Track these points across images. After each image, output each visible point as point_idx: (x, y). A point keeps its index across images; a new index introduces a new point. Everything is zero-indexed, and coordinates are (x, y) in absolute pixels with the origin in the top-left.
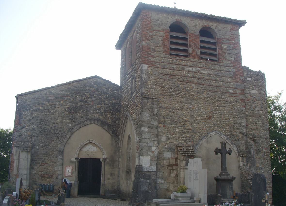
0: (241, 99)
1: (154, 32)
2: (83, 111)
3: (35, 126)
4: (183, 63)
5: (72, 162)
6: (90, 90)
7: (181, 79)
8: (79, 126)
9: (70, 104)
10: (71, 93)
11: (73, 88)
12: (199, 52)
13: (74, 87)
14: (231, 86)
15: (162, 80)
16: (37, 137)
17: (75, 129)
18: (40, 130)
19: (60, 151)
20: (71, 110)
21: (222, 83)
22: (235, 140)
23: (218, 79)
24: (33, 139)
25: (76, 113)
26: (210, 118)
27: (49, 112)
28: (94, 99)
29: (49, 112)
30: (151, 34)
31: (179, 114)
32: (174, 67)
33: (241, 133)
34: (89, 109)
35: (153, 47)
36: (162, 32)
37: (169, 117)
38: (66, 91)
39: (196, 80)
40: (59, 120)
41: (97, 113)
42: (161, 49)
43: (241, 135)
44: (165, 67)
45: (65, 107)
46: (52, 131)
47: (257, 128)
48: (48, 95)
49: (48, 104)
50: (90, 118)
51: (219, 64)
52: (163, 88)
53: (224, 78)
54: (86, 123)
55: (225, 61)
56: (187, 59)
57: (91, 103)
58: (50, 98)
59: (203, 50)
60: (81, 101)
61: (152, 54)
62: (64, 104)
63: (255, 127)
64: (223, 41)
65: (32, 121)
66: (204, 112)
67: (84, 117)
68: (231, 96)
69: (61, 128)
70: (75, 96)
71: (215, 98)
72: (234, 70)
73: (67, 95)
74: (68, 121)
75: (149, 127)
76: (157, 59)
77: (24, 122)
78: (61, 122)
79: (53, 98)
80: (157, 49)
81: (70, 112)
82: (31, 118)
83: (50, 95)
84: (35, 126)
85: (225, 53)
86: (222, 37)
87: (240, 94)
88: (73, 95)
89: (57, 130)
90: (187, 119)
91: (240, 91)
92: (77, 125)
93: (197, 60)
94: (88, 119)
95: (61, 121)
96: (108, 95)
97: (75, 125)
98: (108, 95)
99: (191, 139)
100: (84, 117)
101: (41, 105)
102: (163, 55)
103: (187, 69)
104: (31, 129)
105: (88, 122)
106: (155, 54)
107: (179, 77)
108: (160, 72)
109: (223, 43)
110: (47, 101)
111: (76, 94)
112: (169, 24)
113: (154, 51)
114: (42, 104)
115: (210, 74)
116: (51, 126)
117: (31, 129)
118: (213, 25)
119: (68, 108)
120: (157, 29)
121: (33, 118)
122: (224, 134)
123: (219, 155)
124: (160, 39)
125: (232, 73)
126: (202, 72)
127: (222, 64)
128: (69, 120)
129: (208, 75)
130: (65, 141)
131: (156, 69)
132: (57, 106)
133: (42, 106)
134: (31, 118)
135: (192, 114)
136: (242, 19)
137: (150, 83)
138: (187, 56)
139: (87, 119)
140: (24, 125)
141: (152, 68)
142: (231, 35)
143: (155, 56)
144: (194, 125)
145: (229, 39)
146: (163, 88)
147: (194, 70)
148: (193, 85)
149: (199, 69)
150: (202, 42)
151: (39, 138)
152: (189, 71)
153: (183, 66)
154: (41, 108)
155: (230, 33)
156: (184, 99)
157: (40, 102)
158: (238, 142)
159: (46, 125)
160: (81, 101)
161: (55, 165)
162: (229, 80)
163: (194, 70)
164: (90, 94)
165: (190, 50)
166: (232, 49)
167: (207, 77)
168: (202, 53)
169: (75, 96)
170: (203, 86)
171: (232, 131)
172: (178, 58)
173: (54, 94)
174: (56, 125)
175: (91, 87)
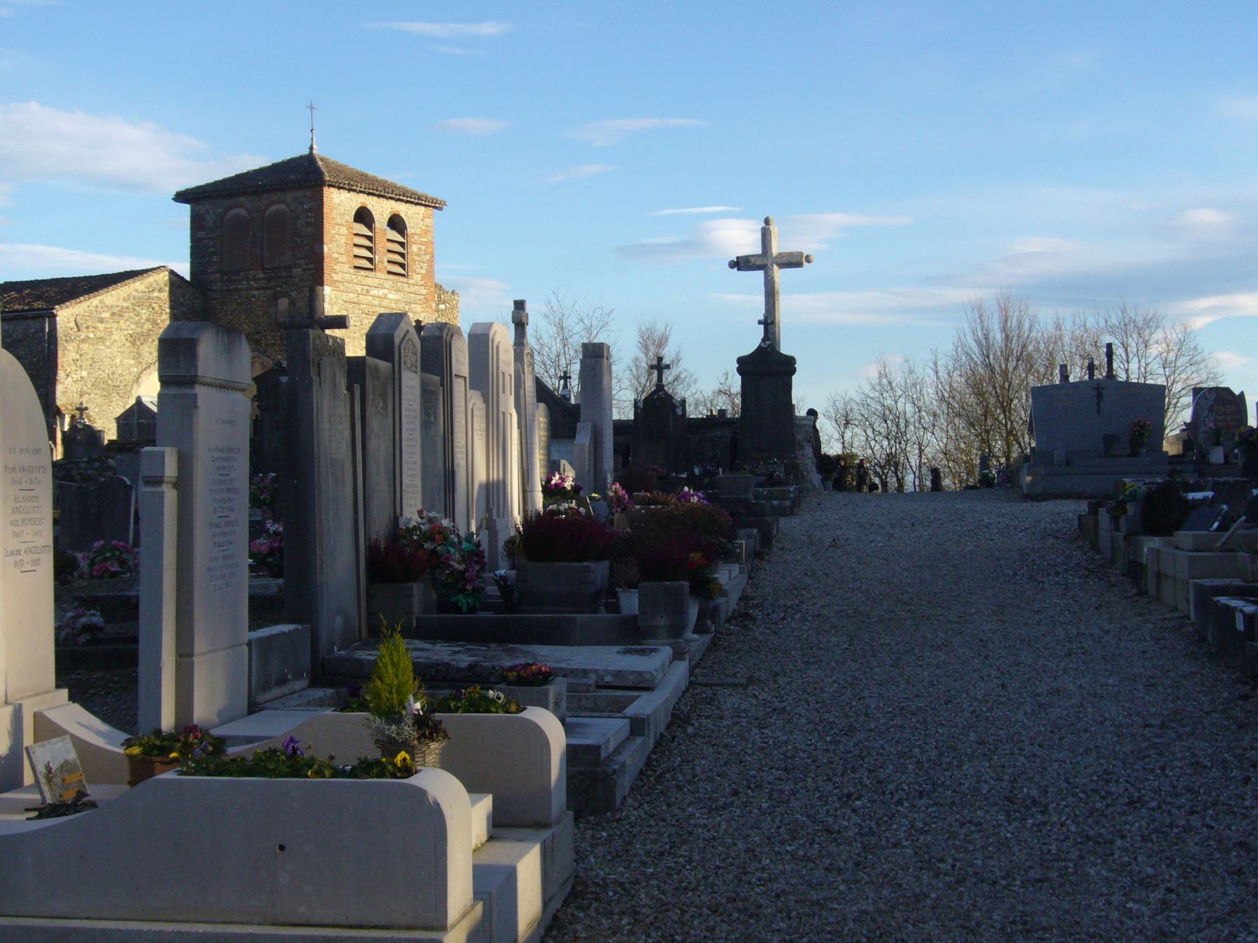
1: (337, 227)
4: (370, 281)
6: (159, 298)
9: (133, 326)
13: (136, 291)
16: (89, 394)
20: (135, 340)
25: (142, 344)
29: (104, 344)
42: (344, 259)
44: (350, 290)
46: (110, 382)
49: (101, 326)
56: (373, 273)
60: (148, 320)
62: (124, 327)
64: (413, 240)
65: (79, 363)
69: (121, 375)
72: (424, 292)
73: (127, 308)
74: (132, 362)
77: (69, 366)
81: (133, 344)
82: (78, 357)
84: (84, 374)
85: (416, 261)
88: (137, 308)
92: (145, 369)
95: (121, 361)
96: (184, 309)
98: (184, 309)
101: (91, 329)
102: (346, 268)
103: (372, 293)
104: (79, 379)
107: (364, 306)
110: (99, 322)
111: (139, 306)
113: (337, 261)
114: (93, 327)
115: (399, 300)
116: (107, 371)
117: (79, 379)
120: (338, 221)
121: (81, 355)
124: (343, 241)
125: (423, 297)
126: (391, 296)
128: (133, 359)
129: (397, 301)
131: (339, 293)
133: (93, 332)
134: (78, 357)
136: (440, 197)
141: (334, 292)
142: (423, 228)
145: (420, 236)
149: (385, 291)
151: (92, 396)
153: (368, 288)
154: (91, 335)
157: (89, 324)
159: (99, 369)
164: (160, 306)
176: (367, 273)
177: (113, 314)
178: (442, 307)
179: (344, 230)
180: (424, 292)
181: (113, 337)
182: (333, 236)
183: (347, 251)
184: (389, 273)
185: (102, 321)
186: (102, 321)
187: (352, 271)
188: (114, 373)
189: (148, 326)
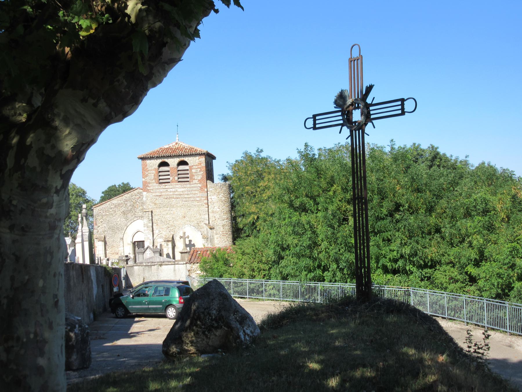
0: (205, 203)
2: (132, 212)
3: (105, 225)
5: (129, 244)
7: (166, 197)
8: (131, 222)
10: (124, 202)
11: (125, 198)
12: (176, 178)
14: (198, 196)
15: (155, 200)
17: (129, 224)
18: (109, 227)
19: (121, 238)
21: (192, 195)
22: (201, 228)
23: (189, 193)
24: (105, 233)
26: (184, 217)
27: (112, 215)
28: (138, 203)
29: (112, 215)
30: (147, 173)
31: (166, 217)
32: (161, 190)
33: (205, 224)
34: (136, 210)
35: (149, 181)
36: (154, 170)
37: (160, 220)
38: (121, 201)
39: (175, 196)
40: (118, 220)
41: (141, 212)
42: (154, 181)
43: (205, 225)
45: (121, 211)
46: (115, 227)
47: (215, 219)
48: (110, 205)
49: (111, 210)
50: (137, 216)
51: (189, 183)
52: (155, 204)
53: (193, 192)
54: (135, 219)
55: (194, 181)
56: (169, 184)
57: (136, 206)
58: (112, 207)
59: (180, 176)
60: (130, 206)
61: (148, 185)
63: (214, 219)
64: (192, 168)
65: (103, 222)
66: (180, 214)
67: (133, 216)
68: (198, 202)
70: (126, 203)
71: (187, 205)
72: (200, 185)
73: (122, 203)
74: (124, 220)
75: (147, 227)
76: (151, 188)
78: (120, 220)
79: (113, 206)
80: (151, 181)
82: (103, 220)
83: (111, 204)
86: (193, 164)
87: (204, 200)
89: (118, 226)
90: (170, 219)
91: (204, 198)
93: (176, 184)
94: (136, 217)
97: (128, 221)
99: (173, 230)
100: (133, 216)
102: (155, 184)
105: (136, 219)
106: (150, 185)
108: (153, 195)
109: (192, 169)
112: (157, 164)
113: (149, 183)
116: (114, 223)
118: (186, 159)
119: (123, 211)
120: (151, 169)
122: (193, 226)
123: (182, 239)
126: (179, 190)
127: (192, 183)
130: (124, 232)
131: (151, 193)
132: (116, 211)
134: (103, 220)
135: (173, 216)
137: (148, 202)
138: (169, 182)
139: (136, 217)
140: (99, 225)
142: (199, 162)
143: (150, 186)
144: (175, 222)
146: (155, 204)
147: (174, 190)
148: (173, 199)
149: (177, 189)
150: (178, 171)
152: (171, 192)
154: (107, 213)
155: (198, 160)
156: (168, 209)
157: (106, 210)
158: (203, 229)
160: (130, 206)
161: (119, 247)
162: (196, 192)
163: (174, 190)
165: (171, 178)
166: (199, 171)
167: (182, 193)
168: (179, 178)
169: (126, 203)
170: (179, 199)
171: (198, 224)
172: (164, 184)
173: (114, 204)
174: (117, 222)
175: (135, 196)
176: (166, 184)
177: (115, 206)
178: (211, 189)
179: (154, 172)
180: (200, 185)
181: (116, 213)
182: (147, 175)
183: (154, 179)
184: (179, 182)
185: (111, 208)
186: (111, 208)
187: (158, 185)
188: (117, 224)
189: (130, 208)
